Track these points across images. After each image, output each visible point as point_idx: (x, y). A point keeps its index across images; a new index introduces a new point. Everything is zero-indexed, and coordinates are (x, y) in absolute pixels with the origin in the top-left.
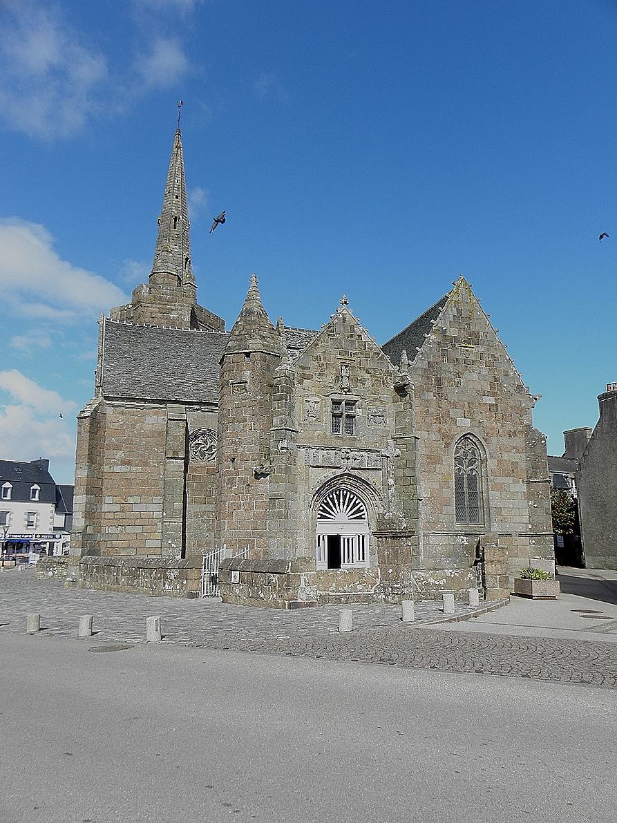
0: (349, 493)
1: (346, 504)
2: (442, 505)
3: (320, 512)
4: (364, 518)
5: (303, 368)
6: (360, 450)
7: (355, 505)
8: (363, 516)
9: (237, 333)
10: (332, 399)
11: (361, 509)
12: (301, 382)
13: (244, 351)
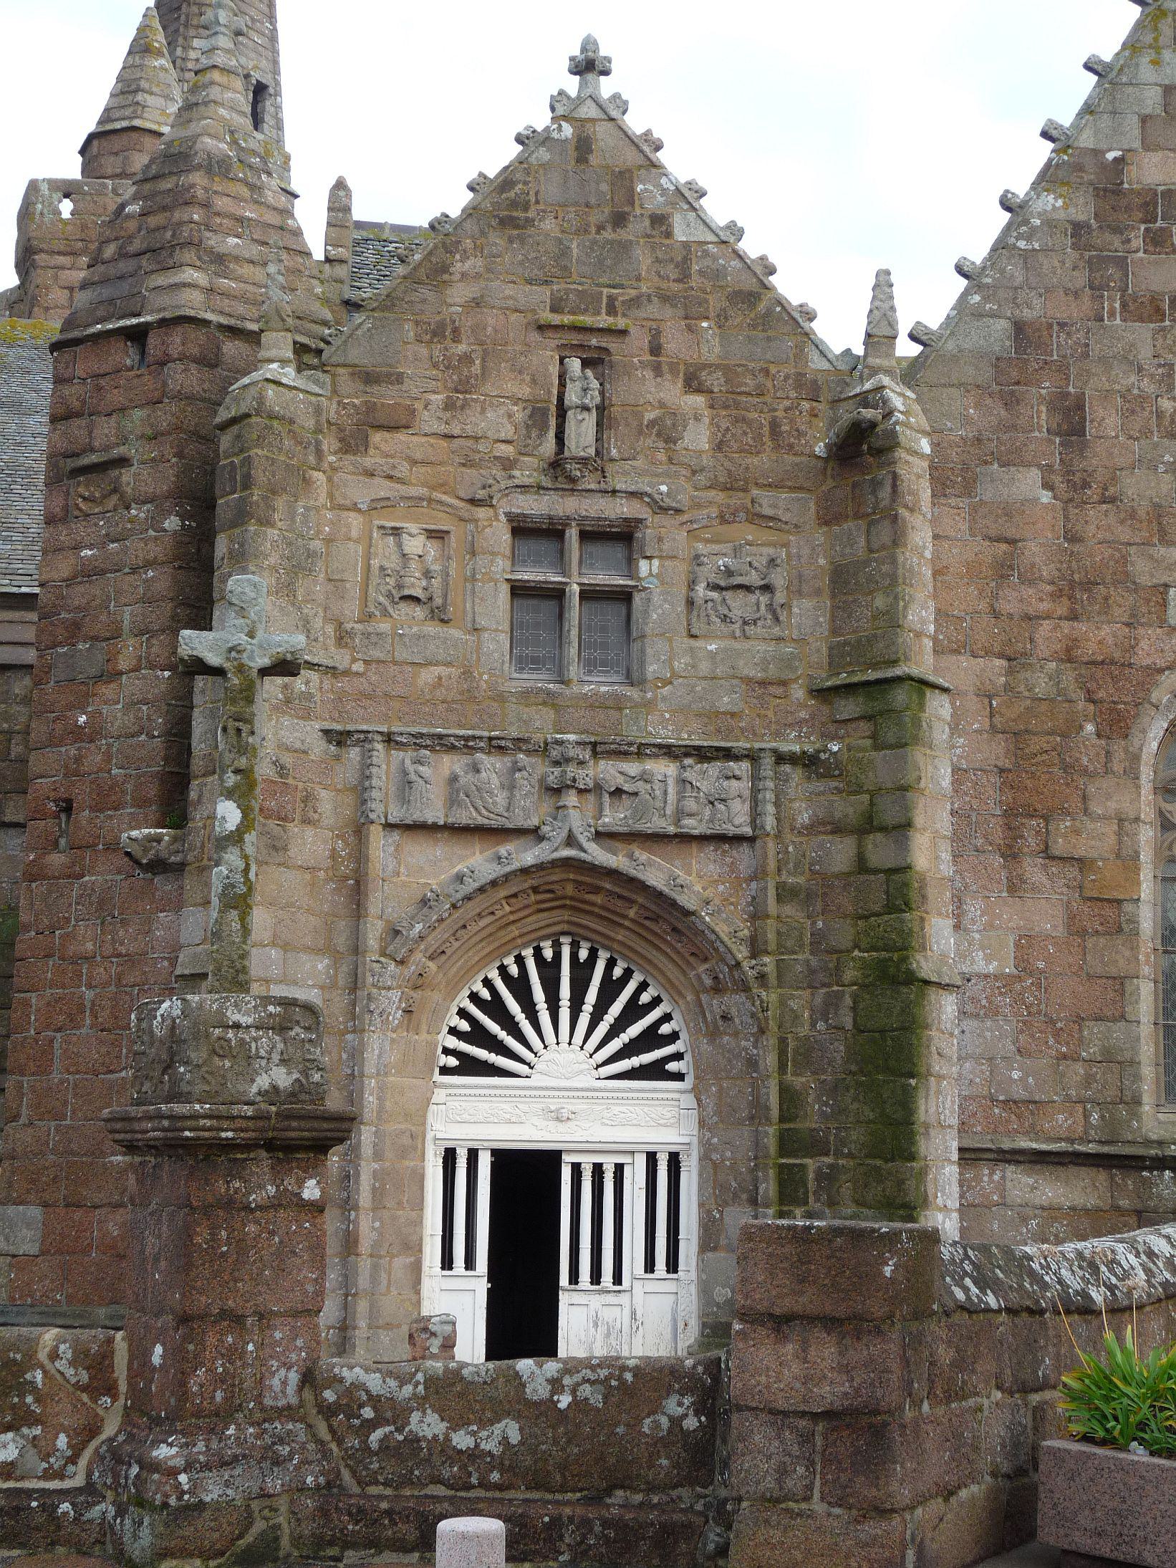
0: (603, 957)
1: (565, 1003)
2: (1079, 1020)
3: (452, 1042)
4: (679, 1077)
5: (369, 378)
6: (640, 752)
7: (633, 1011)
8: (672, 1066)
9: (110, 251)
10: (511, 518)
11: (665, 1029)
12: (353, 443)
13: (122, 323)
